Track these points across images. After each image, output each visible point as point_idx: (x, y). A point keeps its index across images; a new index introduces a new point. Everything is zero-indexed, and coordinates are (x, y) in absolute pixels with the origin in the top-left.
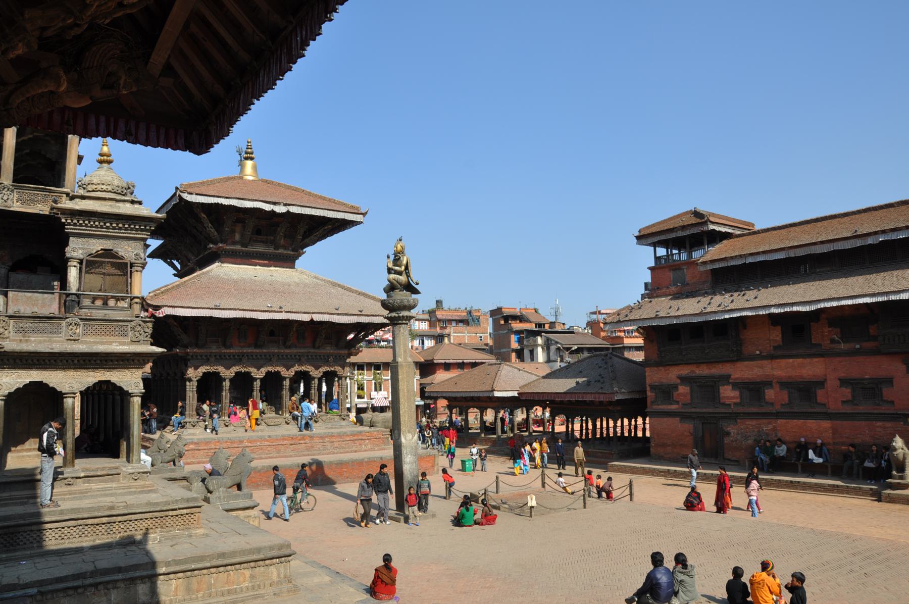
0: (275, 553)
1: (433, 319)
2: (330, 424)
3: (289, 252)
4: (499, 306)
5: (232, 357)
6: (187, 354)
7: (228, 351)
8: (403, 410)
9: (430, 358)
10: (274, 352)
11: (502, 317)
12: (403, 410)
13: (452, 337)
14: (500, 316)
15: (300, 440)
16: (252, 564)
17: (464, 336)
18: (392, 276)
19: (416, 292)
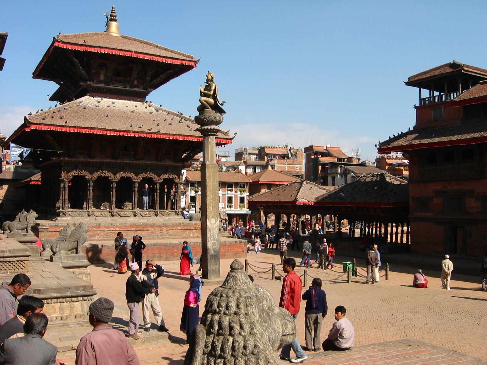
0: (80, 292)
1: (263, 154)
2: (167, 217)
3: (141, 90)
4: (311, 144)
5: (94, 165)
6: (61, 161)
7: (91, 161)
8: (209, 201)
9: (257, 180)
10: (127, 163)
11: (313, 153)
12: (209, 201)
13: (276, 167)
14: (311, 152)
15: (143, 228)
16: (61, 300)
17: (285, 167)
18: (204, 98)
19: (222, 111)
